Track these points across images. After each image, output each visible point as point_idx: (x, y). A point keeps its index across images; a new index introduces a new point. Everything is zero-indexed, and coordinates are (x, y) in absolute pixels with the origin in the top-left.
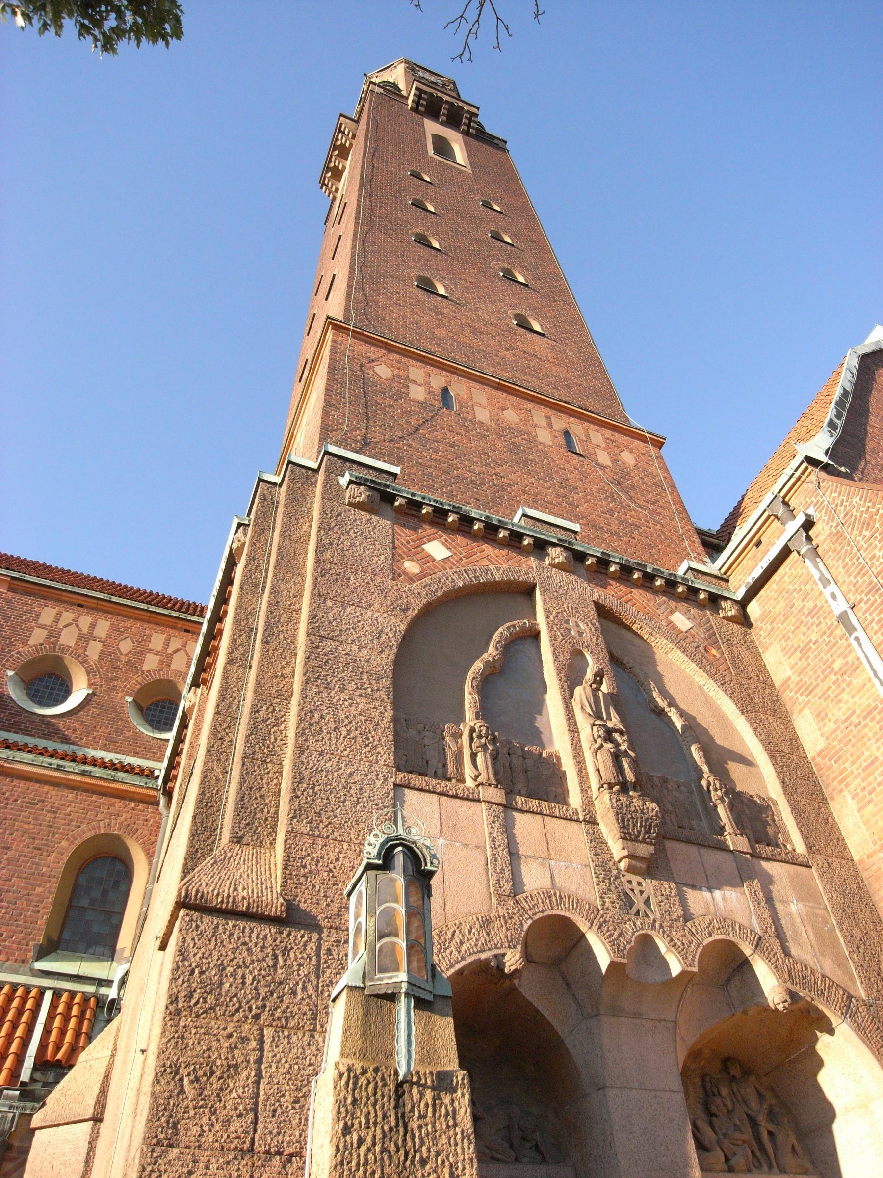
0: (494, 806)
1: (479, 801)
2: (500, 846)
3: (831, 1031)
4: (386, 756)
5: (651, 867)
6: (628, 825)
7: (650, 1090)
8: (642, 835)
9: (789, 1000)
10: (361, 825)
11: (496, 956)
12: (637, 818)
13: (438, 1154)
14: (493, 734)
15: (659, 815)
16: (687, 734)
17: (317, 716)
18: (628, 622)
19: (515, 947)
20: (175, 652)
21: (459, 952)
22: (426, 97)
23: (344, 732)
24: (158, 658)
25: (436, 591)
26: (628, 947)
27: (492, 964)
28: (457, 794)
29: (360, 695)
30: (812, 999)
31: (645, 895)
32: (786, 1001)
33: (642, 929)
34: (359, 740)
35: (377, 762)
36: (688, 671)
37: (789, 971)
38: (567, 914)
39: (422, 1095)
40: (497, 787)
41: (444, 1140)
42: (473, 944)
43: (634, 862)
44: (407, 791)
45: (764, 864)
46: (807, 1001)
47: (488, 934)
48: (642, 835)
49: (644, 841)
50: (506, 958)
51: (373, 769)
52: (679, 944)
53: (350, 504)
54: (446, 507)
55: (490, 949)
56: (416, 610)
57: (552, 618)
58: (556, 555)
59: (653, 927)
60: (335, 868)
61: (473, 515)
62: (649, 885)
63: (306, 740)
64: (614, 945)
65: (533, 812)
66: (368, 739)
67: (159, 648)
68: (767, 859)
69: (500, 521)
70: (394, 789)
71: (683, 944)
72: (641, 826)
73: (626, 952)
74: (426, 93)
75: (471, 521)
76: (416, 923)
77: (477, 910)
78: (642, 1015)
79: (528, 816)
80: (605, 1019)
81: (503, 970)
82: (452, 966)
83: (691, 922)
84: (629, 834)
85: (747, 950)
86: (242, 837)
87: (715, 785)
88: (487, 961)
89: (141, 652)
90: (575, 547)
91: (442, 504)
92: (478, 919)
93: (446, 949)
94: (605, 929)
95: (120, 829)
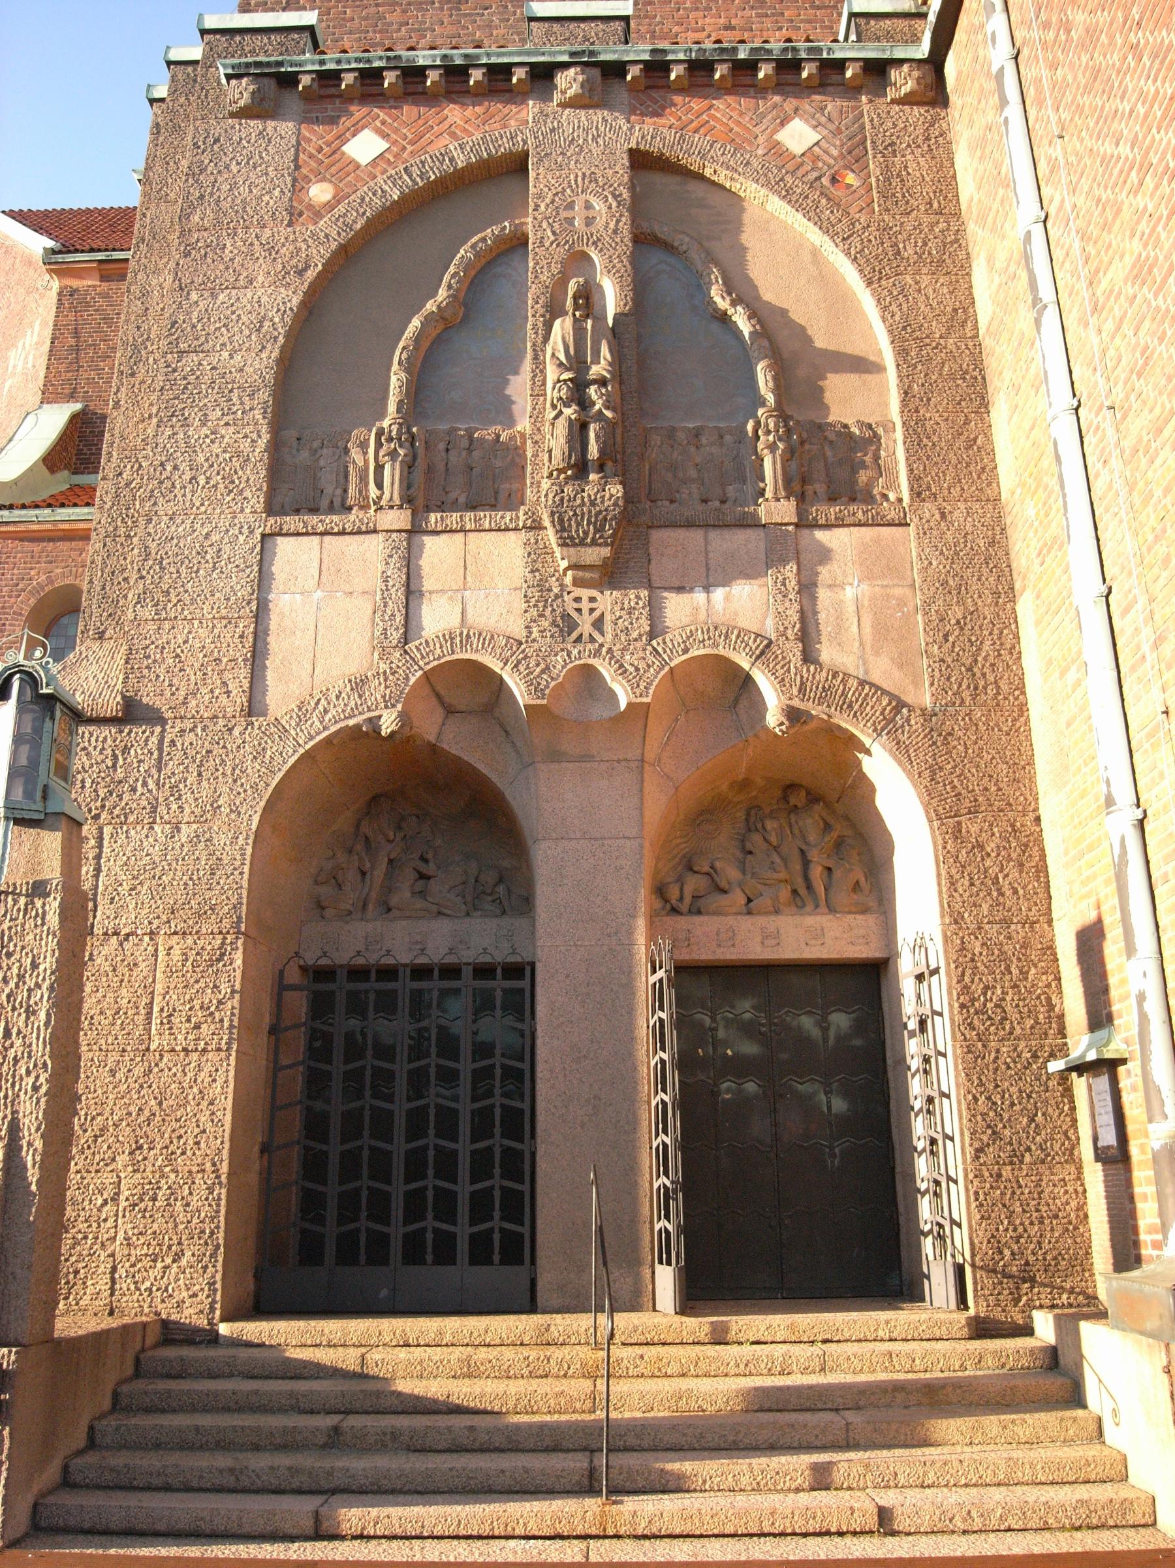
0: (394, 535)
1: (375, 531)
4: (256, 500)
5: (611, 575)
7: (596, 839)
10: (217, 595)
11: (370, 719)
12: (583, 514)
13: (23, 948)
14: (409, 431)
15: (620, 503)
16: (755, 346)
17: (169, 468)
19: (393, 706)
23: (202, 480)
25: (355, 222)
26: (553, 684)
29: (227, 424)
31: (597, 614)
32: (782, 724)
34: (221, 486)
35: (242, 510)
37: (802, 683)
38: (473, 657)
39: (15, 902)
40: (401, 507)
41: (31, 936)
44: (279, 539)
45: (819, 535)
47: (360, 696)
49: (594, 543)
50: (383, 720)
52: (632, 669)
53: (233, 115)
54: (376, 64)
56: (320, 267)
57: (543, 208)
58: (568, 82)
59: (597, 653)
61: (421, 62)
62: (607, 600)
63: (155, 504)
65: (451, 531)
66: (233, 482)
68: (828, 526)
69: (466, 56)
70: (262, 541)
71: (637, 669)
75: (421, 72)
76: (25, 749)
77: (353, 670)
79: (444, 537)
80: (542, 766)
82: (312, 738)
83: (660, 639)
84: (572, 538)
85: (744, 663)
86: (103, 632)
87: (767, 425)
88: (358, 727)
90: (602, 58)
91: (369, 61)
94: (521, 668)
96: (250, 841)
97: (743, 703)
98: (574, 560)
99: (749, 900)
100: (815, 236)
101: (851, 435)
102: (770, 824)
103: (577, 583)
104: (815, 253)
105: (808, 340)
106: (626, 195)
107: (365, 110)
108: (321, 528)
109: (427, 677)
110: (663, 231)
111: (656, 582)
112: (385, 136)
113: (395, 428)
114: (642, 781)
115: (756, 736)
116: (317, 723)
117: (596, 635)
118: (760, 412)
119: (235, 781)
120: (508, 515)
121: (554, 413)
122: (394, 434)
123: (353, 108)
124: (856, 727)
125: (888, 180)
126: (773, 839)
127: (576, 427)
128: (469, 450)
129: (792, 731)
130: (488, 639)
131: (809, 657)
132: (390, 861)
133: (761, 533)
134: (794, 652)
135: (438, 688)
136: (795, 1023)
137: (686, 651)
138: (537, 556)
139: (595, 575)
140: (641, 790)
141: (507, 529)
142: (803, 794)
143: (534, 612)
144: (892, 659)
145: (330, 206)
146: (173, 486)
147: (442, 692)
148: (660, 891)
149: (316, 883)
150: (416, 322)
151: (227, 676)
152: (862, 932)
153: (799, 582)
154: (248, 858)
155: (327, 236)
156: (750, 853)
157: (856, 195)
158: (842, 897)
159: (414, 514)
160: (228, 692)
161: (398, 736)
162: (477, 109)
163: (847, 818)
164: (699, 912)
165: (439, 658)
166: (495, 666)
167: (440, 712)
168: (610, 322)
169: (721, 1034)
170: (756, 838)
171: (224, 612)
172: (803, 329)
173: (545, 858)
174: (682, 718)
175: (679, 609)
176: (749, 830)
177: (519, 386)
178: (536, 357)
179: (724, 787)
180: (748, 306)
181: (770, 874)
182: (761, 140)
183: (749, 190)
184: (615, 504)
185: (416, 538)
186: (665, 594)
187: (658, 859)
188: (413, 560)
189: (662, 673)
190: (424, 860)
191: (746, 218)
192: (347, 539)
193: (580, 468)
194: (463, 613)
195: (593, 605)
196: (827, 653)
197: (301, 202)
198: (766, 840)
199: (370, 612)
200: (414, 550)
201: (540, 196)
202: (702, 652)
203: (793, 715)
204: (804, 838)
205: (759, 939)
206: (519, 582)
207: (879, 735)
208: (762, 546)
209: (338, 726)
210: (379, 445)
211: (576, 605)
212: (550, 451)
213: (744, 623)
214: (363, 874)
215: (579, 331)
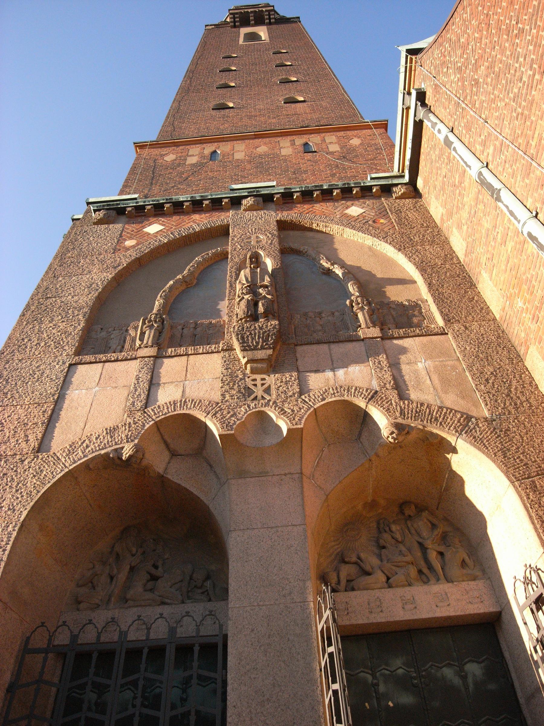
0: (146, 359)
1: (136, 358)
2: (143, 381)
3: (454, 450)
5: (273, 366)
6: (248, 340)
7: (272, 528)
8: (260, 344)
9: (395, 431)
11: (116, 450)
12: (255, 334)
15: (277, 327)
16: (346, 278)
17: (26, 340)
18: (308, 225)
19: (132, 441)
21: (83, 453)
22: (238, 16)
23: (42, 344)
25: (145, 250)
26: (238, 422)
27: (111, 456)
28: (117, 358)
29: (63, 322)
30: (424, 426)
32: (392, 433)
33: (256, 408)
35: (61, 355)
36: (359, 240)
40: (152, 346)
42: (97, 445)
43: (255, 365)
44: (79, 366)
45: (395, 342)
46: (419, 429)
47: (111, 437)
48: (260, 344)
49: (262, 348)
51: (57, 359)
52: (289, 411)
53: (95, 224)
55: (110, 446)
56: (125, 265)
57: (236, 239)
59: (267, 404)
60: (6, 421)
61: (181, 200)
62: (271, 379)
63: (14, 355)
64: (225, 424)
66: (60, 343)
69: (202, 196)
71: (293, 411)
72: (259, 338)
73: (234, 426)
74: (237, 13)
75: (181, 203)
78: (268, 472)
79: (176, 358)
80: (233, 481)
81: (122, 459)
82: (75, 462)
83: (306, 395)
84: (249, 346)
85: (362, 404)
88: (107, 454)
90: (262, 193)
91: (158, 201)
92: (106, 429)
93: (73, 453)
94: (218, 415)
96: (17, 529)
97: (365, 434)
98: (251, 357)
99: (388, 578)
100: (369, 241)
101: (404, 306)
102: (394, 528)
103: (253, 371)
104: (370, 248)
105: (374, 276)
106: (275, 233)
107: (155, 219)
108: (104, 359)
109: (158, 425)
110: (295, 246)
111: (301, 368)
112: (163, 225)
113: (153, 316)
114: (302, 487)
115: (377, 455)
116: (80, 454)
117: (266, 396)
118: (352, 298)
119: (17, 491)
120: (213, 346)
121: (239, 299)
122: (152, 319)
123: (150, 219)
124: (443, 431)
125: (400, 220)
126: (398, 536)
127: (252, 303)
128: (195, 328)
129: (401, 438)
130: (197, 403)
131: (402, 396)
132: (132, 569)
133: (362, 343)
134: (393, 396)
135: (166, 437)
136: (439, 674)
137: (323, 399)
138: (230, 363)
139: (264, 365)
140: (302, 493)
141: (212, 352)
142: (413, 507)
143: (227, 387)
144: (457, 395)
145: (133, 247)
146: (26, 347)
147: (169, 441)
148: (323, 578)
149: (78, 586)
150: (171, 282)
151: (29, 431)
152: (476, 594)
153: (388, 362)
154: (12, 539)
155: (130, 255)
156: (384, 547)
157: (386, 225)
158: (455, 571)
159: (159, 349)
160: (27, 441)
161: (134, 460)
162: (206, 215)
163: (446, 519)
164: (353, 589)
165: (166, 414)
166: (201, 416)
167: (166, 455)
168: (270, 271)
169: (382, 688)
170: (386, 536)
171: (37, 400)
172: (370, 272)
173: (235, 543)
174: (326, 450)
175: (316, 381)
176: (380, 532)
177: (223, 306)
178: (231, 286)
179: (360, 507)
180: (339, 265)
181: (400, 558)
182: (337, 213)
183: (334, 229)
184: (274, 328)
185: (159, 361)
186: (308, 374)
187: (319, 555)
188: (156, 370)
189: (309, 412)
190: (156, 567)
191: (335, 240)
192: (119, 363)
193: (253, 317)
194: (183, 392)
195: (264, 382)
196: (414, 395)
197: (120, 246)
198: (393, 538)
199: (126, 395)
200: (157, 365)
201: (235, 236)
202: (334, 399)
203: (398, 427)
204: (419, 535)
205: (400, 605)
206: (219, 375)
207: (460, 434)
208: (363, 349)
209: (94, 455)
210: (144, 323)
211: (253, 383)
212: (237, 315)
213: (358, 384)
214: (112, 578)
215: (253, 272)
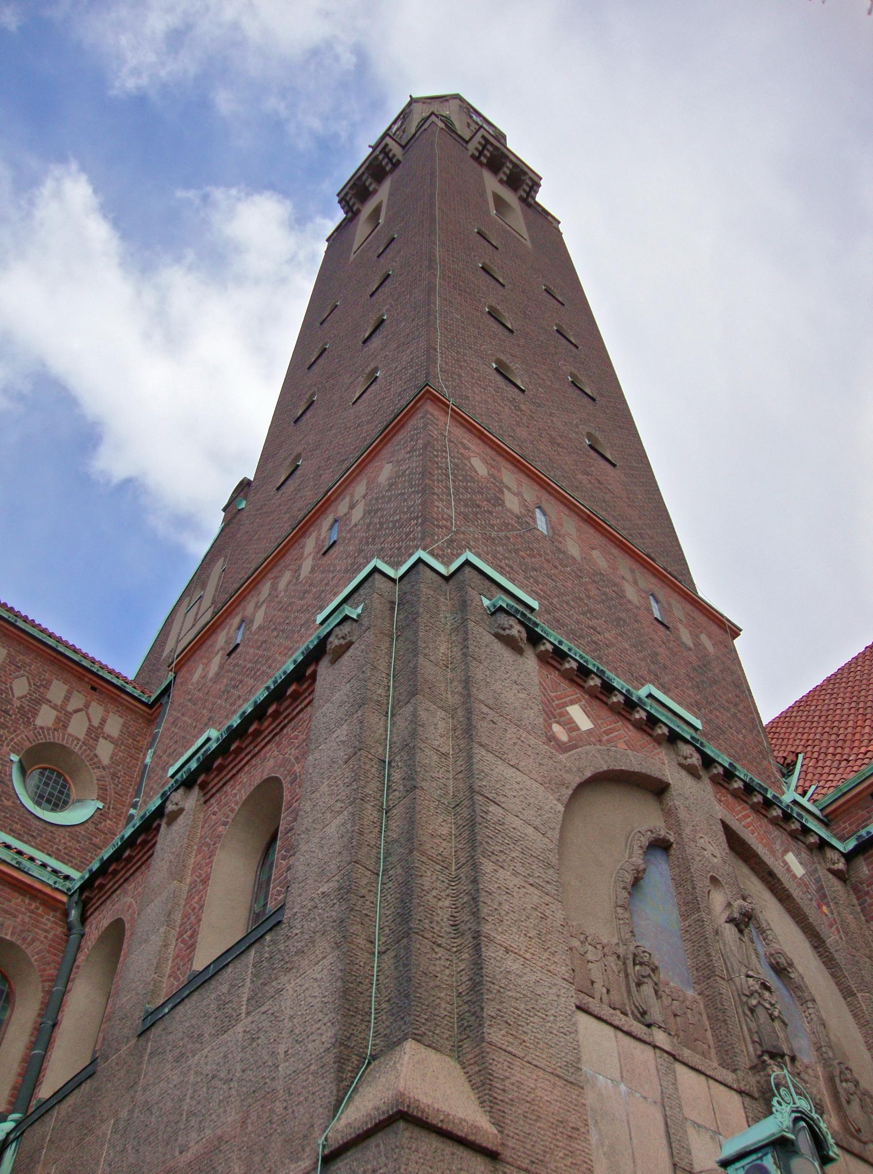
20: (76, 711)
22: (491, 149)
24: (54, 713)
54: (590, 667)
61: (615, 684)
67: (59, 702)
74: (492, 144)
89: (37, 700)
91: (586, 661)
95: (13, 933)
